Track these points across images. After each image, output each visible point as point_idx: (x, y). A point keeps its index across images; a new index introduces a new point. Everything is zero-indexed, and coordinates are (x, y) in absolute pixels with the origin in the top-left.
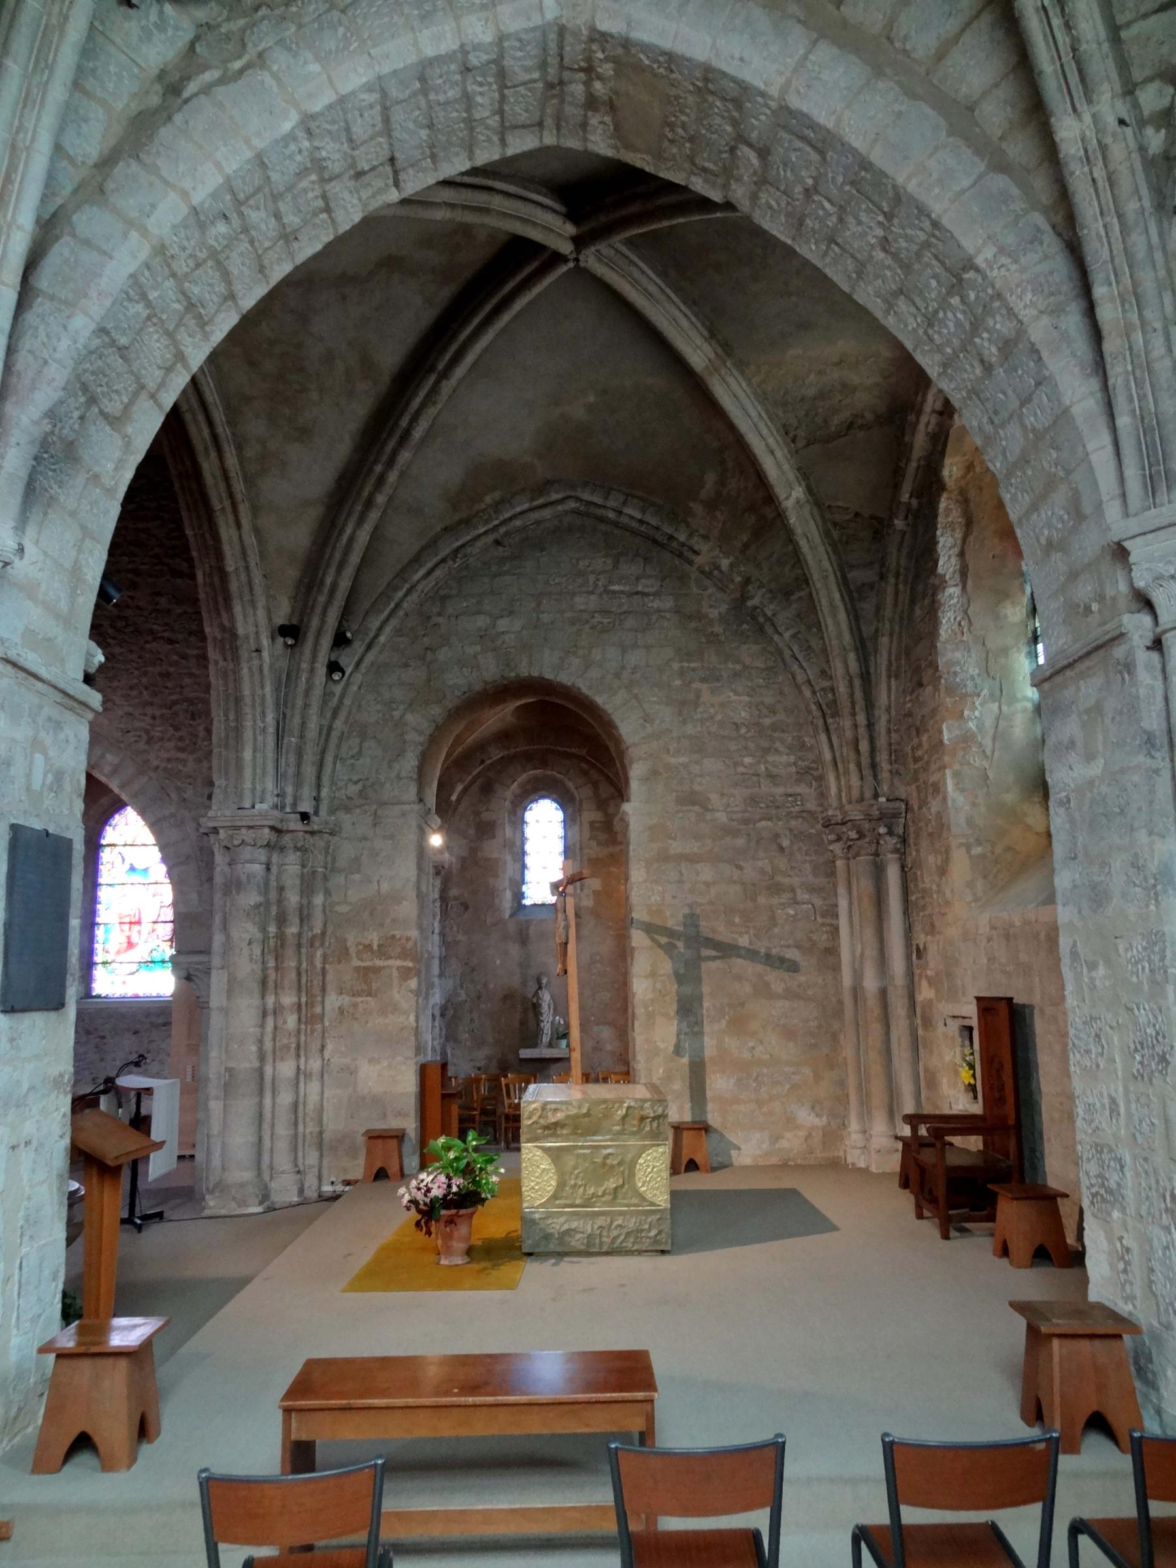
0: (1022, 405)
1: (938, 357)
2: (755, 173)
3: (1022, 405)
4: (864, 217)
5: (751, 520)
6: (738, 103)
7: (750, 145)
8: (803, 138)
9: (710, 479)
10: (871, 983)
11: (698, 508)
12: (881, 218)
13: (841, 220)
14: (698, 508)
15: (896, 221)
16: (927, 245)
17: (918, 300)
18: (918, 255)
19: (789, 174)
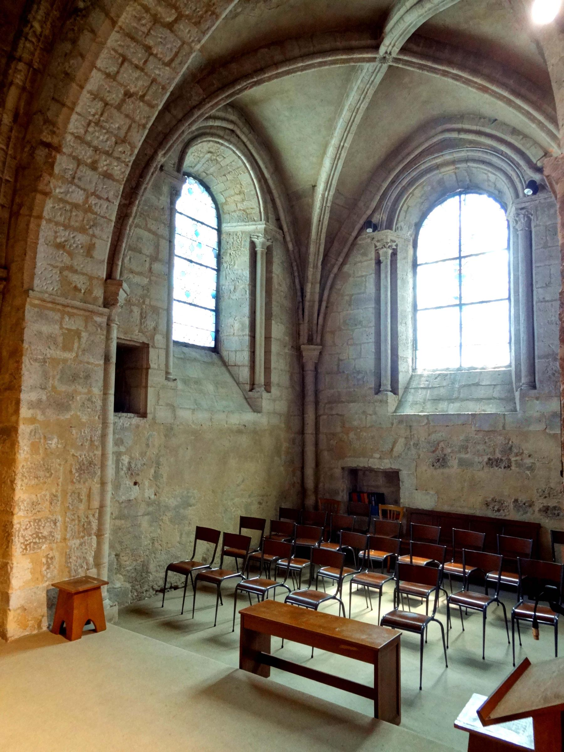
0: (93, 194)
1: (82, 131)
2: (161, 17)
3: (93, 194)
4: (140, 83)
6: (197, 24)
7: (176, 21)
8: (176, 54)
12: (140, 93)
13: (137, 67)
15: (141, 104)
16: (134, 121)
17: (106, 115)
18: (127, 116)
19: (160, 40)
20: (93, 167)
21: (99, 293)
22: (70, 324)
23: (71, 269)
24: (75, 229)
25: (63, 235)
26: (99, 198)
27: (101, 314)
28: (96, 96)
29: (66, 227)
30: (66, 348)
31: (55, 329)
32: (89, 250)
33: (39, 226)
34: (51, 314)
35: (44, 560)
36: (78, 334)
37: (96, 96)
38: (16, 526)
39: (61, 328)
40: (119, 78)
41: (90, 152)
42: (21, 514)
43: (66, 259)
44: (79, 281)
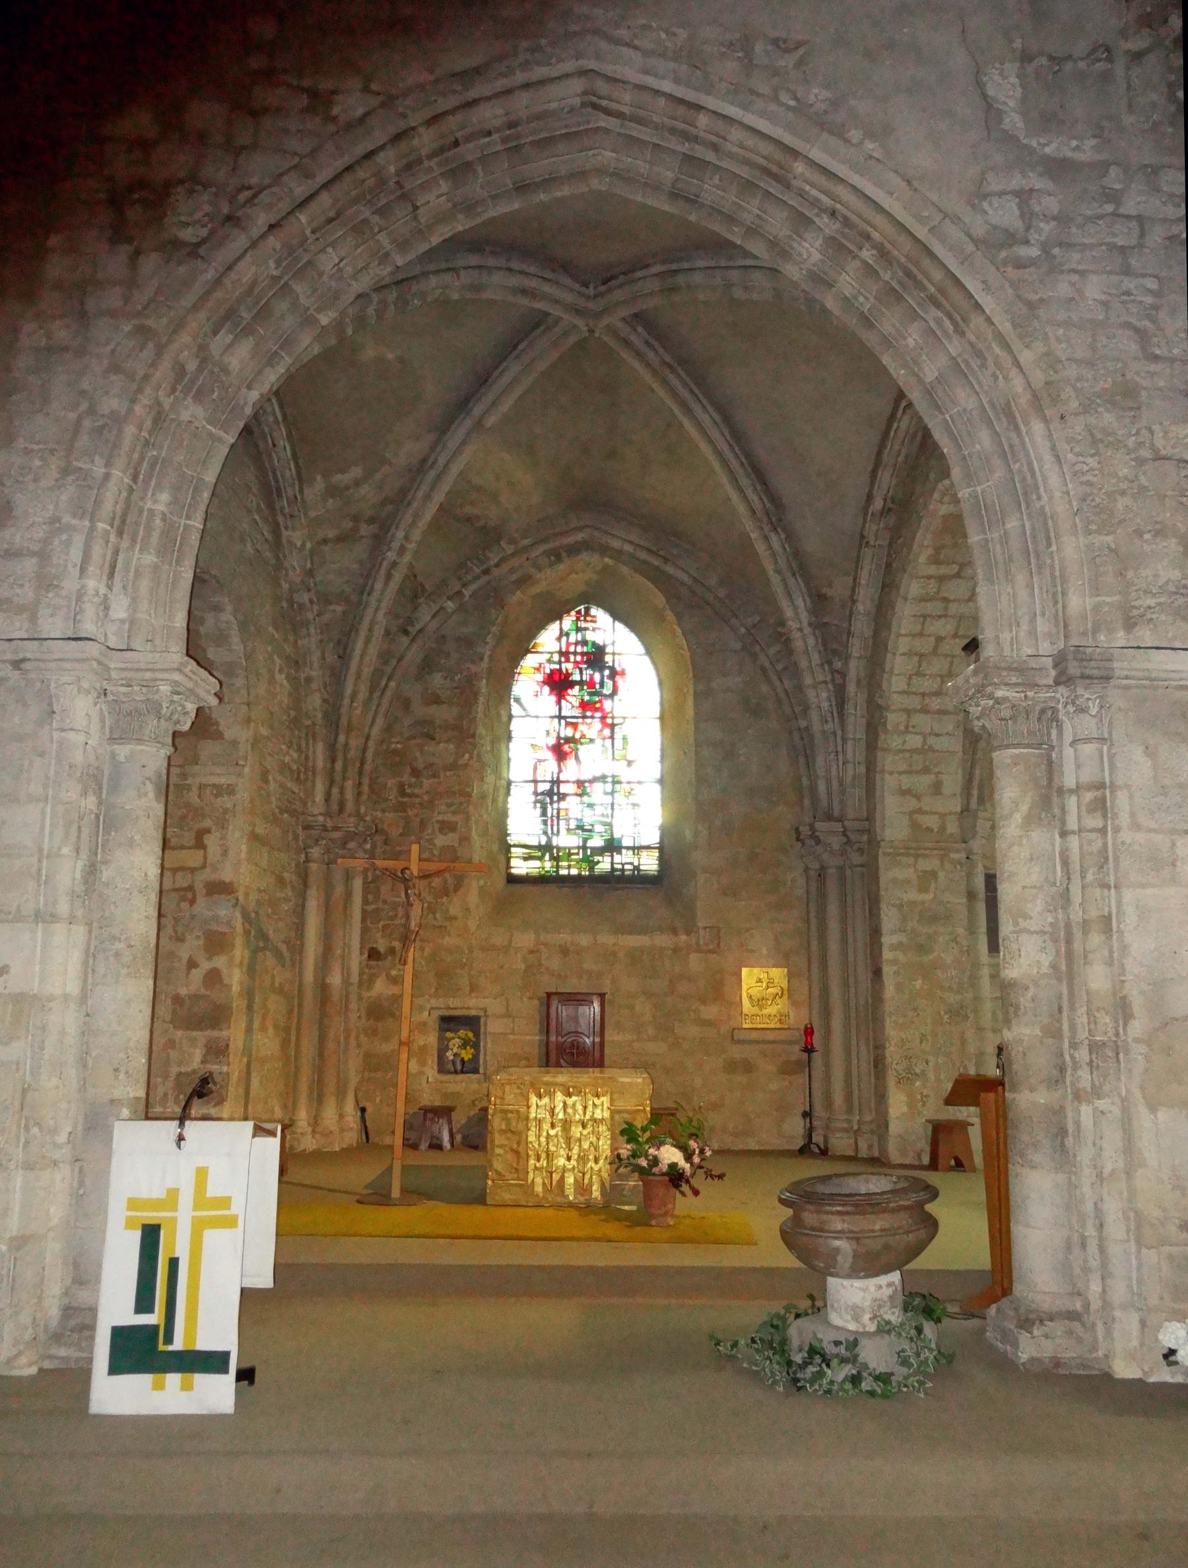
0: (930, 734)
3: (930, 734)
5: (348, 524)
9: (356, 472)
10: (335, 979)
11: (319, 484)
13: (940, 617)
14: (319, 484)
20: (925, 710)
21: (953, 828)
22: (925, 865)
23: (920, 811)
24: (918, 772)
25: (906, 782)
26: (937, 735)
27: (958, 851)
28: (909, 654)
29: (909, 772)
30: (923, 889)
31: (909, 873)
32: (937, 788)
33: (883, 780)
34: (904, 860)
35: (919, 1097)
36: (934, 874)
37: (909, 654)
38: (889, 1060)
39: (916, 871)
40: (926, 632)
41: (918, 699)
42: (892, 1049)
43: (913, 803)
44: (932, 822)
